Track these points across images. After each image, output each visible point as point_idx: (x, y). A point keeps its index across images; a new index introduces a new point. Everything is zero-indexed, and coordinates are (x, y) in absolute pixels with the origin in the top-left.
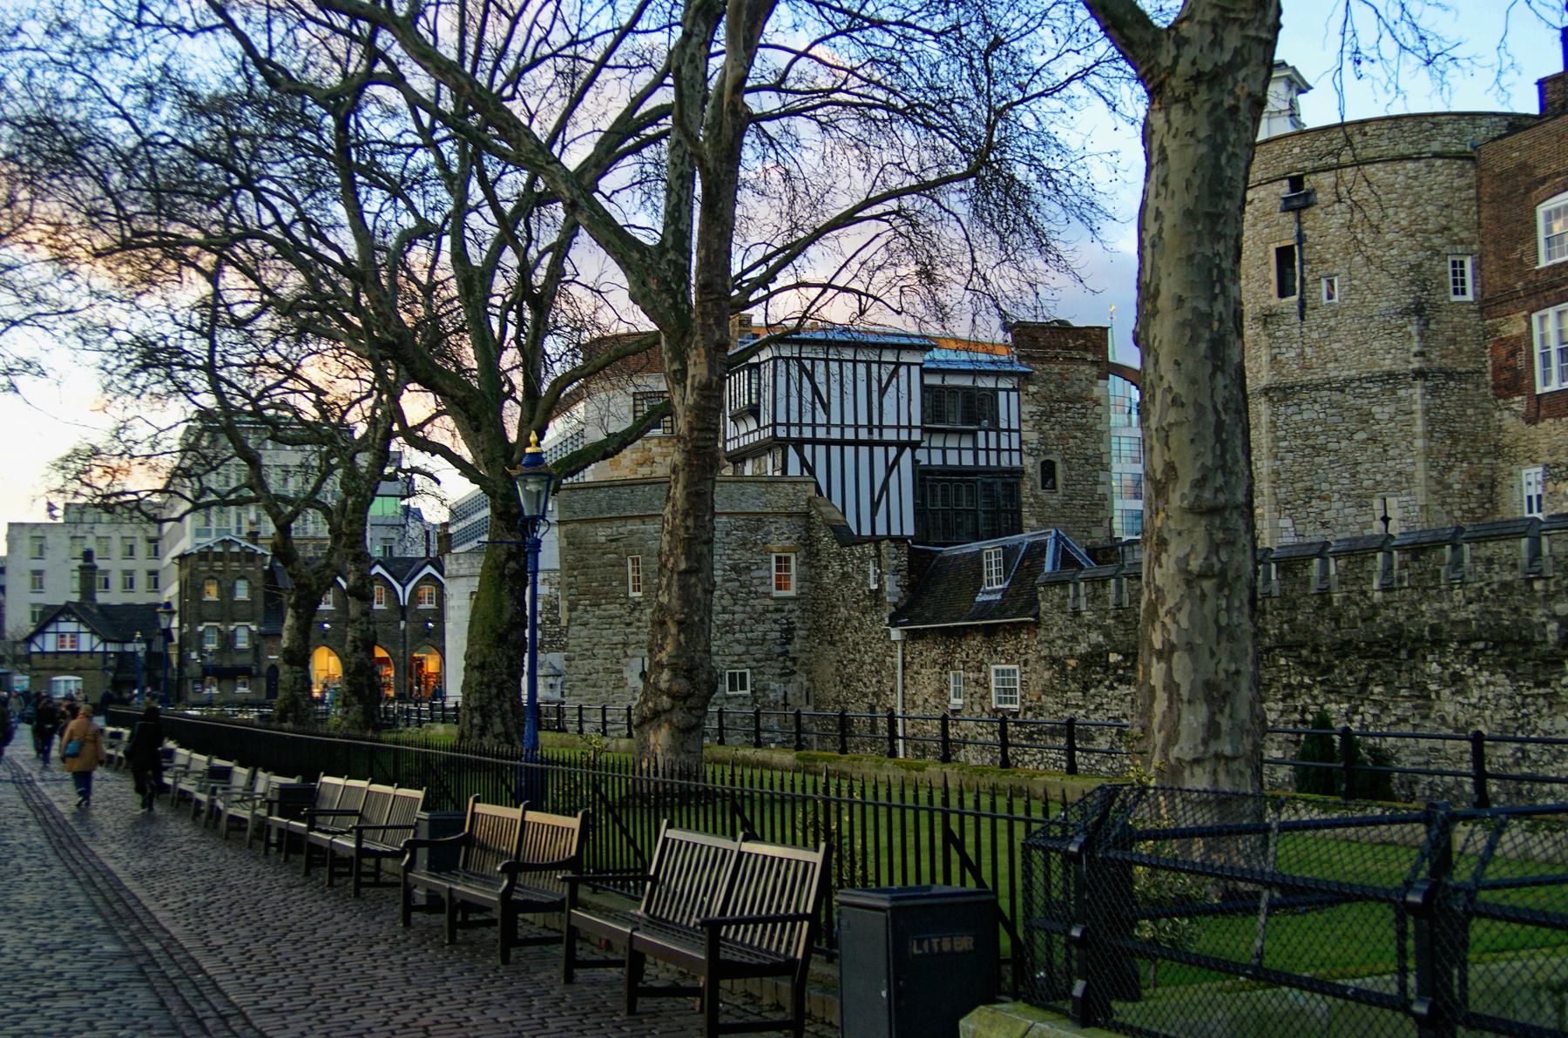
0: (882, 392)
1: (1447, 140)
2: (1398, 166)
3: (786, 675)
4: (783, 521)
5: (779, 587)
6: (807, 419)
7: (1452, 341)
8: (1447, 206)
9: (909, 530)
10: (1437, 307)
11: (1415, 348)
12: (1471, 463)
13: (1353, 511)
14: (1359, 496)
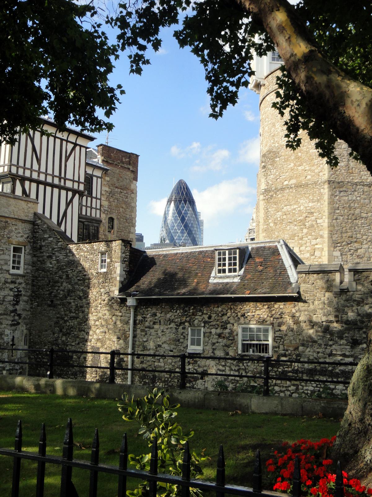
0: (67, 159)
3: (15, 324)
4: (20, 224)
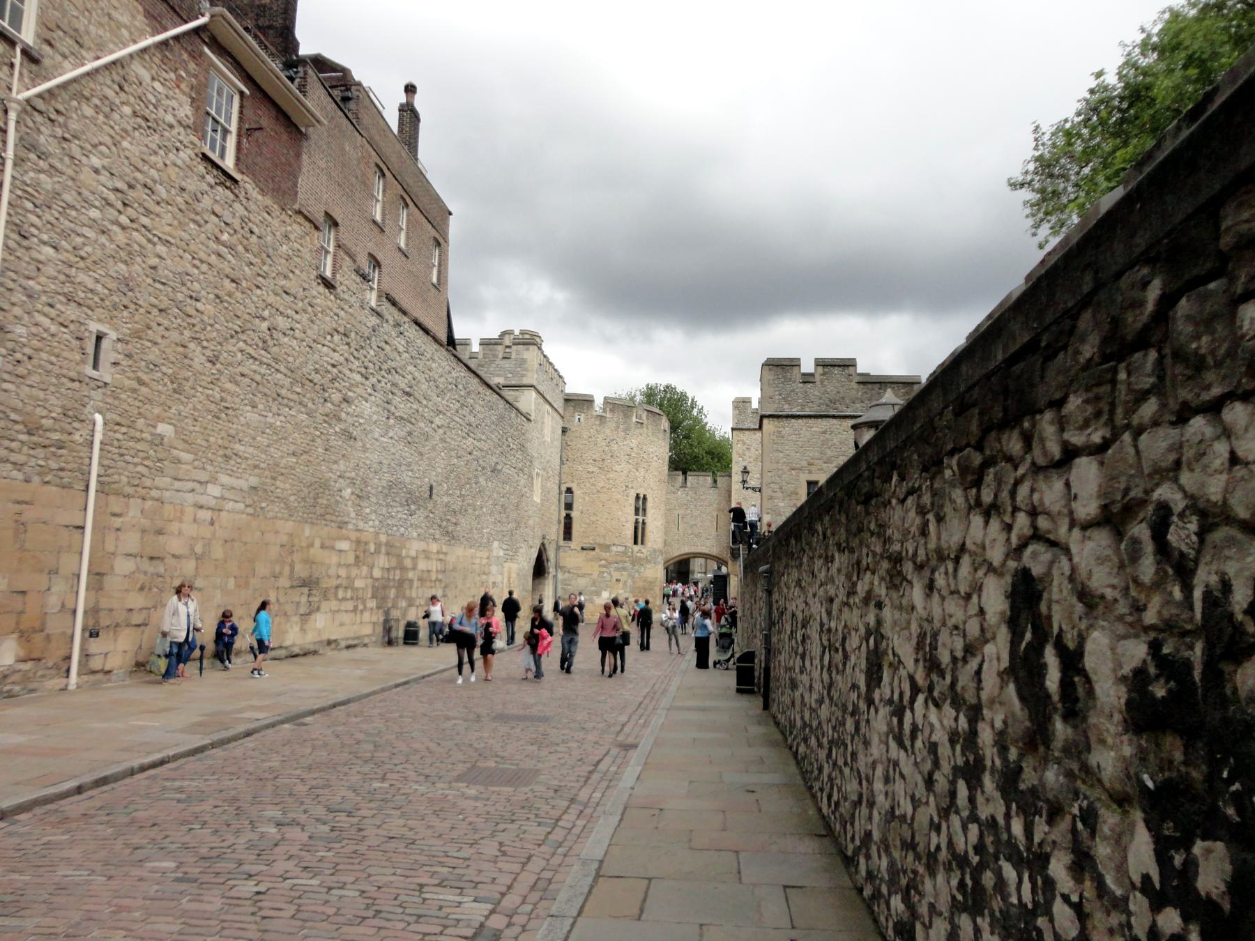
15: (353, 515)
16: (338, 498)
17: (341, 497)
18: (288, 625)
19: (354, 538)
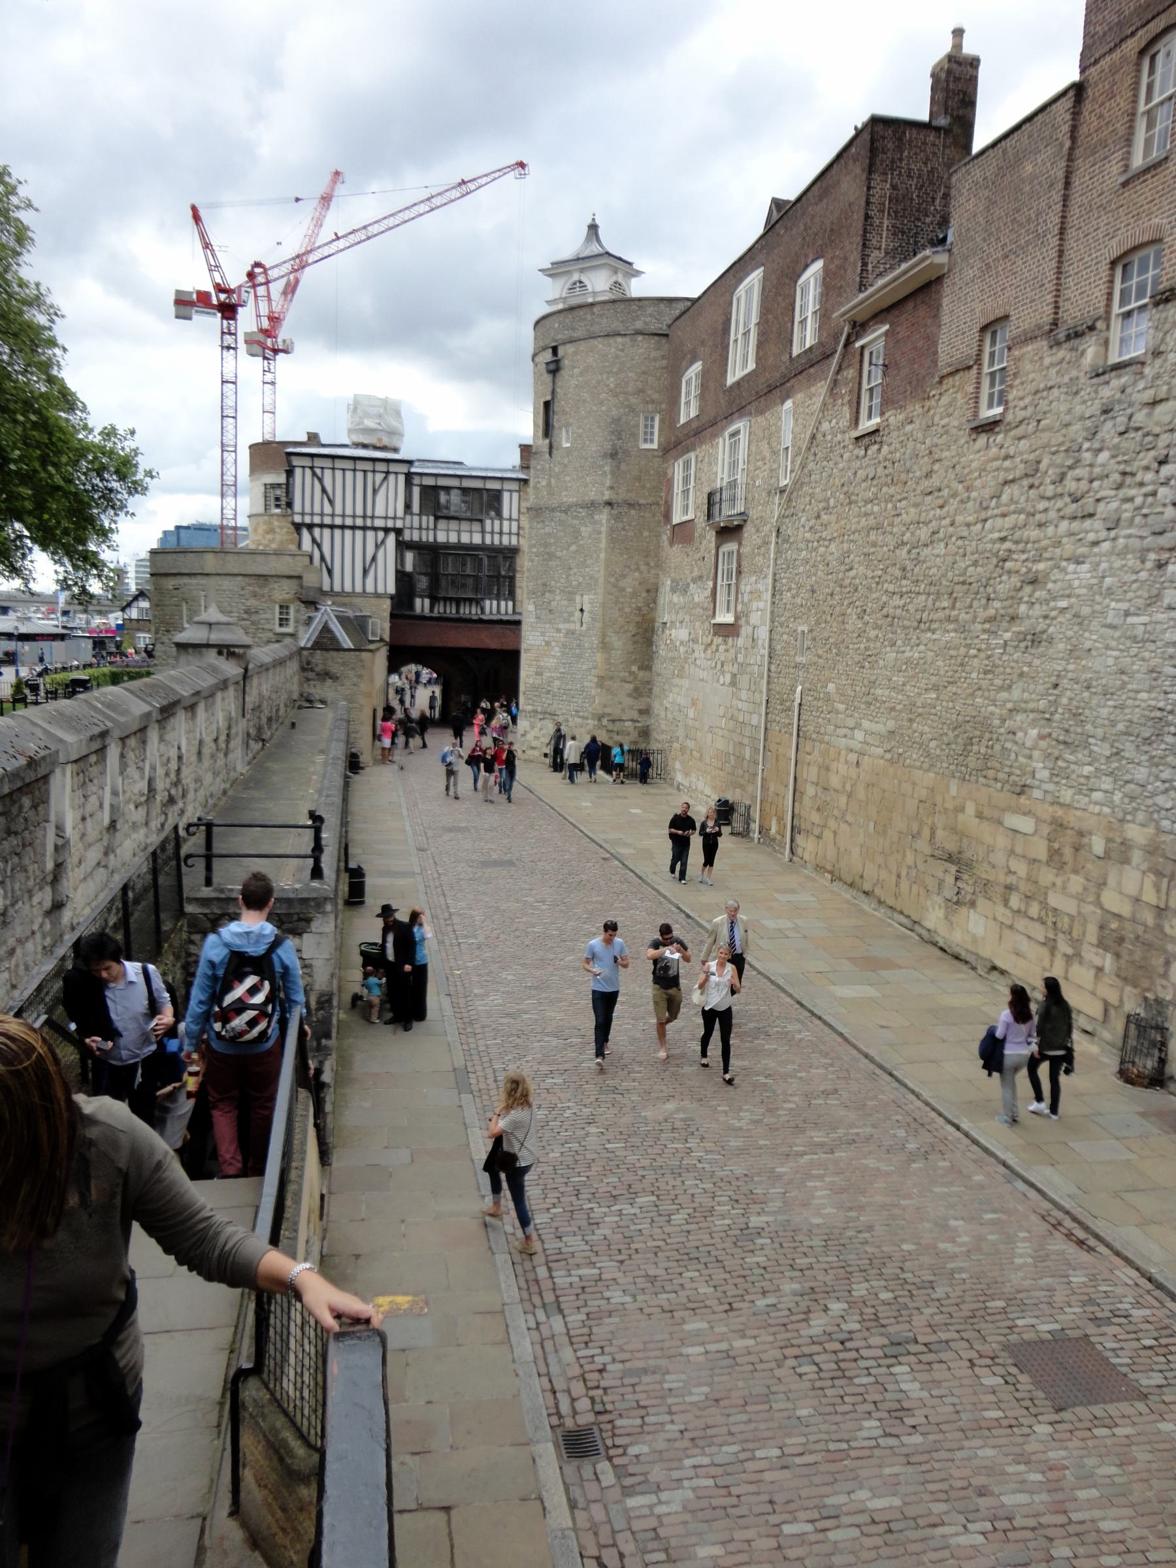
0: (375, 491)
1: (648, 320)
2: (611, 340)
5: (281, 625)
6: (317, 509)
7: (638, 479)
8: (644, 373)
9: (391, 589)
10: (626, 452)
11: (608, 483)
12: (641, 573)
13: (565, 603)
14: (570, 593)
15: (1045, 774)
16: (1009, 745)
17: (1016, 743)
18: (929, 903)
19: (1048, 818)
